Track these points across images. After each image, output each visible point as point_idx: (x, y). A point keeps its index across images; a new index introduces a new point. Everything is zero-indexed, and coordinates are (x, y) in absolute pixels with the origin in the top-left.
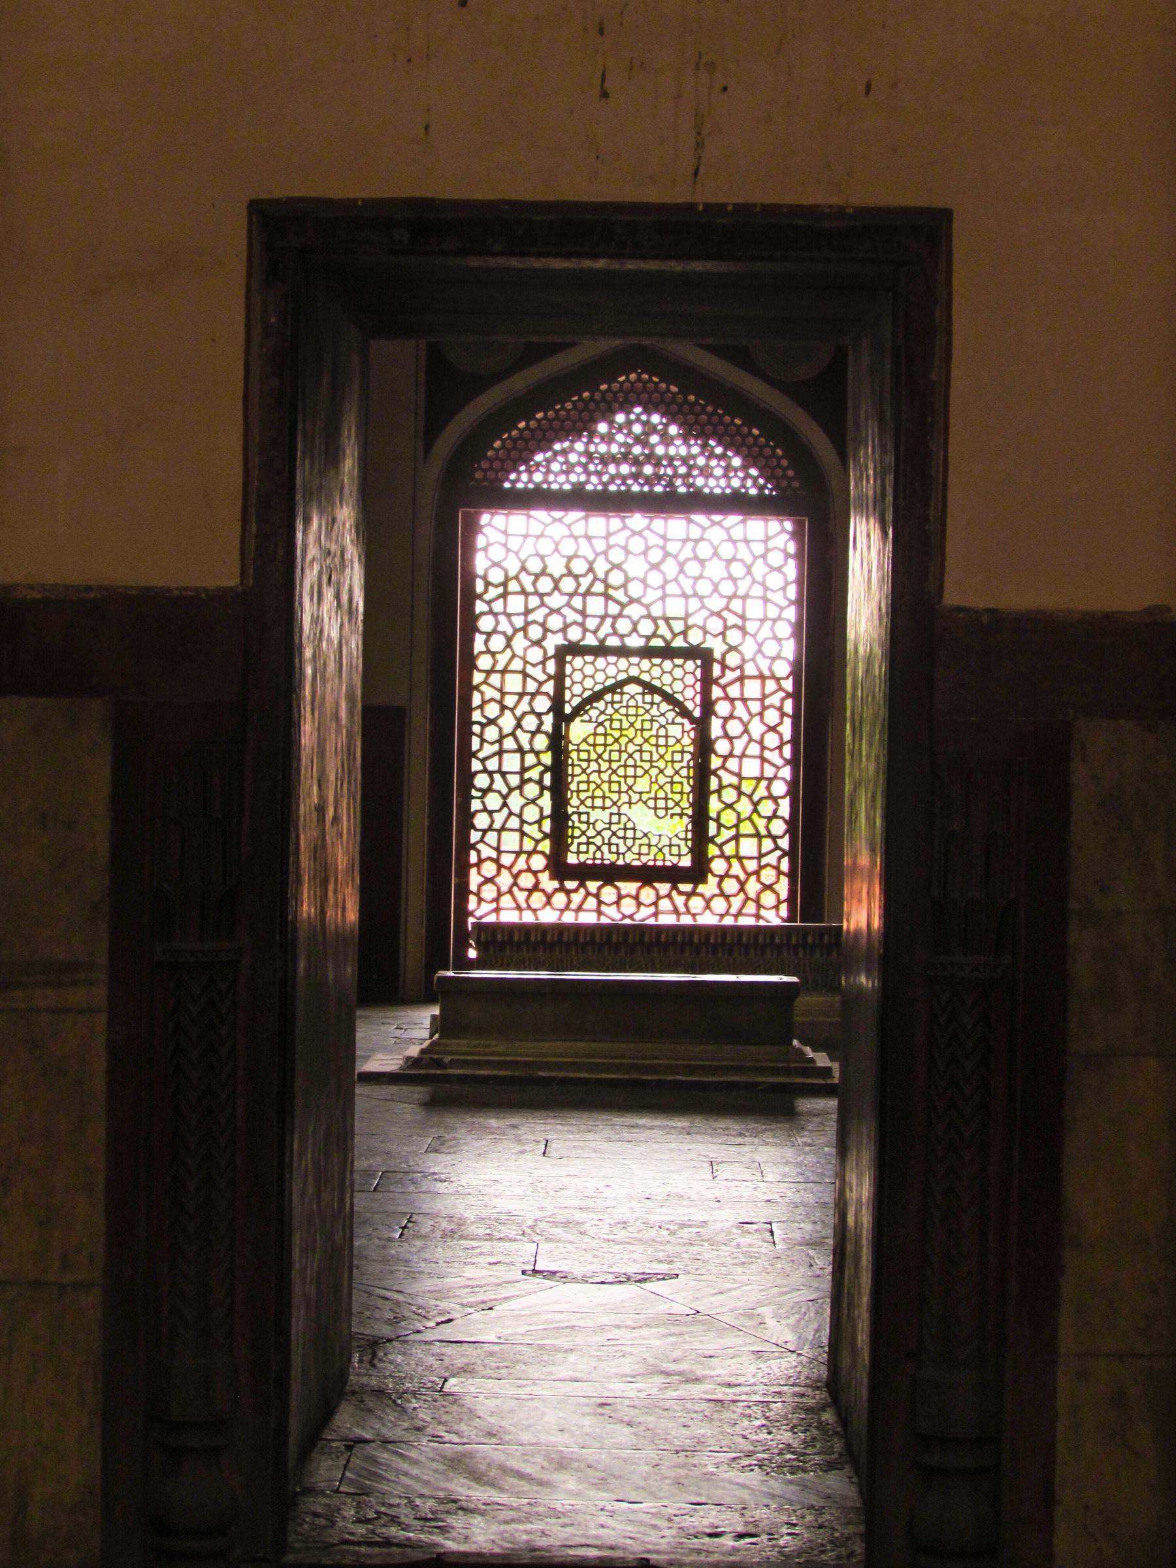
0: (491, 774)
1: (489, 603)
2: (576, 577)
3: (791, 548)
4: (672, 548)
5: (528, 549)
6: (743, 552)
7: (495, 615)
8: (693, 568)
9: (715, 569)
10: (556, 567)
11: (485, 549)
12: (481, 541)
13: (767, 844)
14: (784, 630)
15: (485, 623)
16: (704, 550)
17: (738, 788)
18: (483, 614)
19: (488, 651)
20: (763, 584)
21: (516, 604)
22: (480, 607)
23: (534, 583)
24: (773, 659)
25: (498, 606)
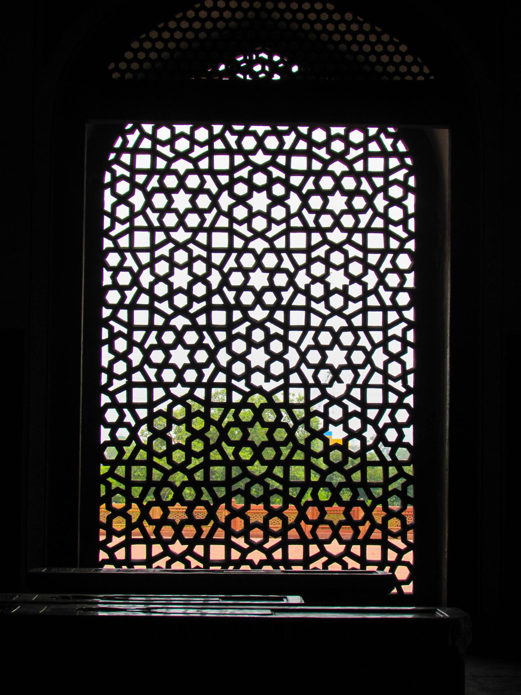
0: (119, 407)
1: (114, 239)
2: (201, 213)
3: (412, 181)
4: (296, 181)
5: (154, 183)
6: (365, 186)
7: (121, 251)
8: (316, 202)
9: (337, 203)
10: (182, 201)
11: (112, 185)
12: (108, 178)
13: (393, 471)
14: (404, 262)
15: (113, 259)
16: (327, 183)
17: (362, 416)
18: (110, 250)
19: (115, 286)
20: (385, 216)
21: (142, 239)
22: (107, 243)
23: (160, 219)
24: (396, 291)
25: (124, 242)
